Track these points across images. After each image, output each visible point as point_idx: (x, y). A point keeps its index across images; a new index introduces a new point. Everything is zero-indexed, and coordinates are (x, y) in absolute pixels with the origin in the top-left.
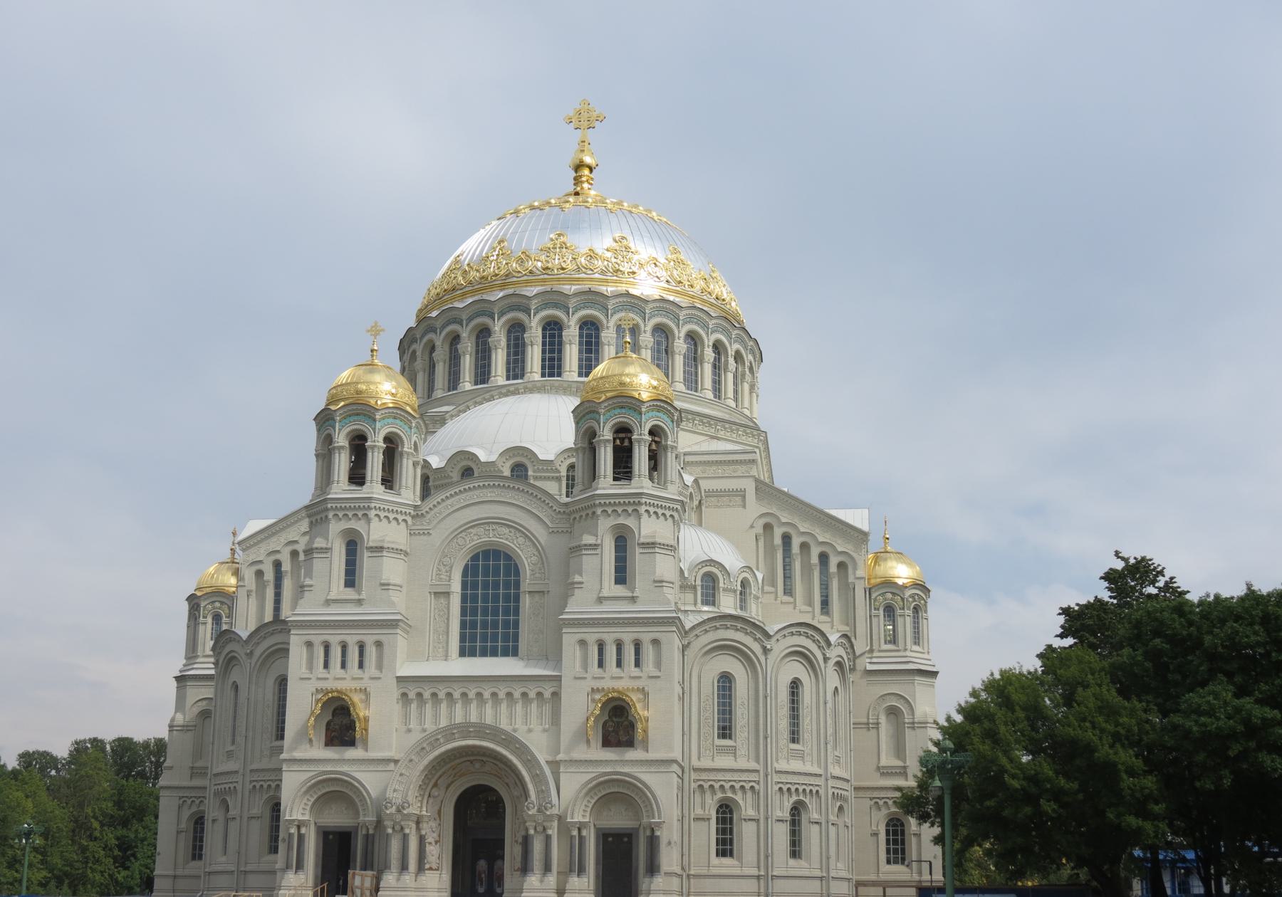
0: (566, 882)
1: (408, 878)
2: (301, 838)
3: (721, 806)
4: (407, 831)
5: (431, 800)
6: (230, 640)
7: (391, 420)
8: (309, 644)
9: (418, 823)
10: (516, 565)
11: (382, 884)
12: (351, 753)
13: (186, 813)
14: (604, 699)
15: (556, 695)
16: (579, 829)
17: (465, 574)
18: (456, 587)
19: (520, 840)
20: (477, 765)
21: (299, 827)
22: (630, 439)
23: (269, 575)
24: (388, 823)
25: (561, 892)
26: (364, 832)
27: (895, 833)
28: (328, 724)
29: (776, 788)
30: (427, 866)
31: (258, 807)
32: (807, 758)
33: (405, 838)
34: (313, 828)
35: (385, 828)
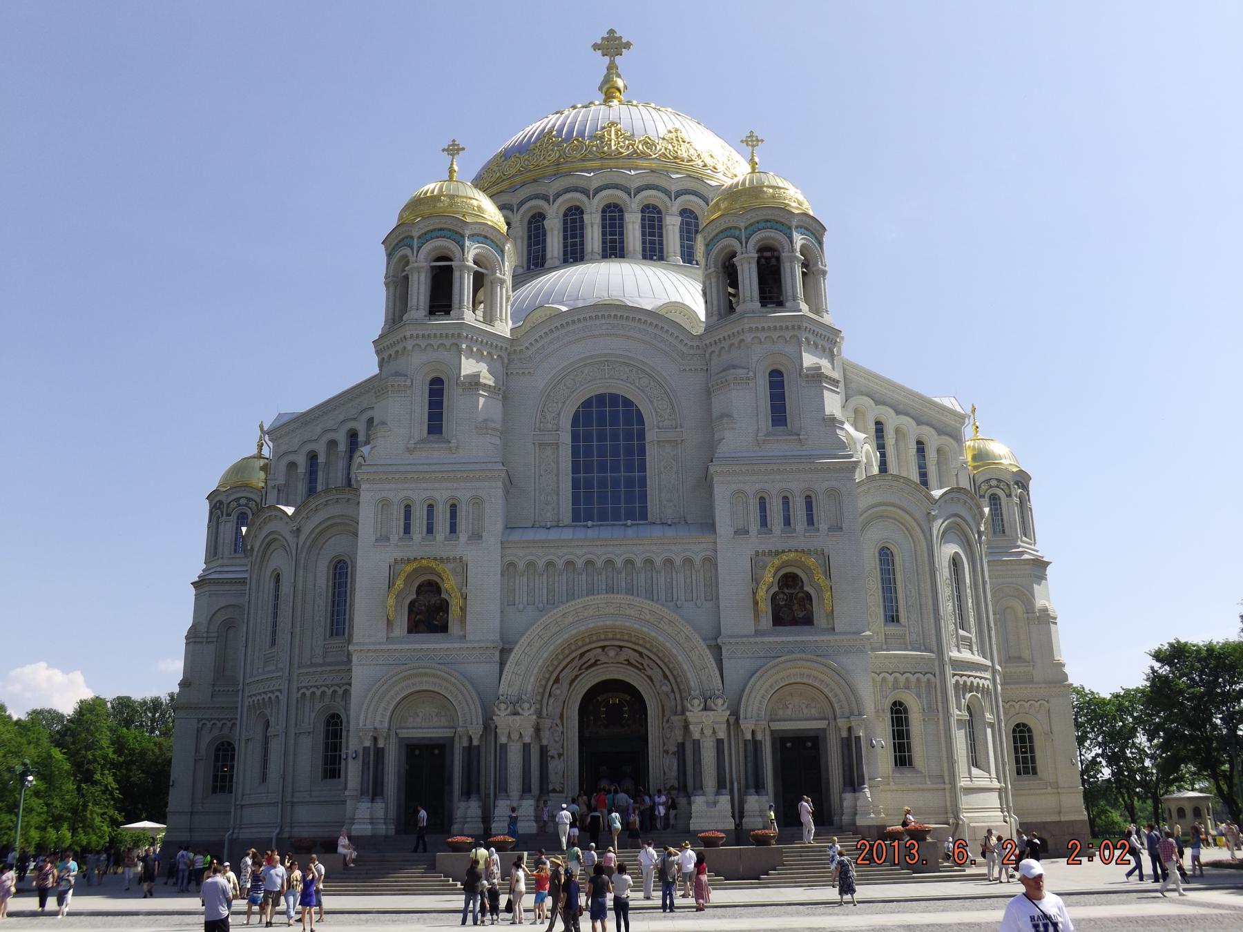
0: (742, 803)
2: (380, 753)
3: (895, 704)
5: (551, 700)
6: (270, 519)
7: (481, 239)
8: (385, 504)
9: (538, 730)
10: (638, 411)
13: (206, 739)
15: (711, 562)
17: (575, 422)
18: (566, 438)
19: (673, 749)
20: (612, 653)
21: (375, 739)
22: (778, 259)
23: (302, 469)
26: (465, 743)
27: (1023, 740)
28: (412, 604)
29: (953, 681)
30: (551, 787)
31: (312, 719)
32: (975, 648)
34: (393, 740)
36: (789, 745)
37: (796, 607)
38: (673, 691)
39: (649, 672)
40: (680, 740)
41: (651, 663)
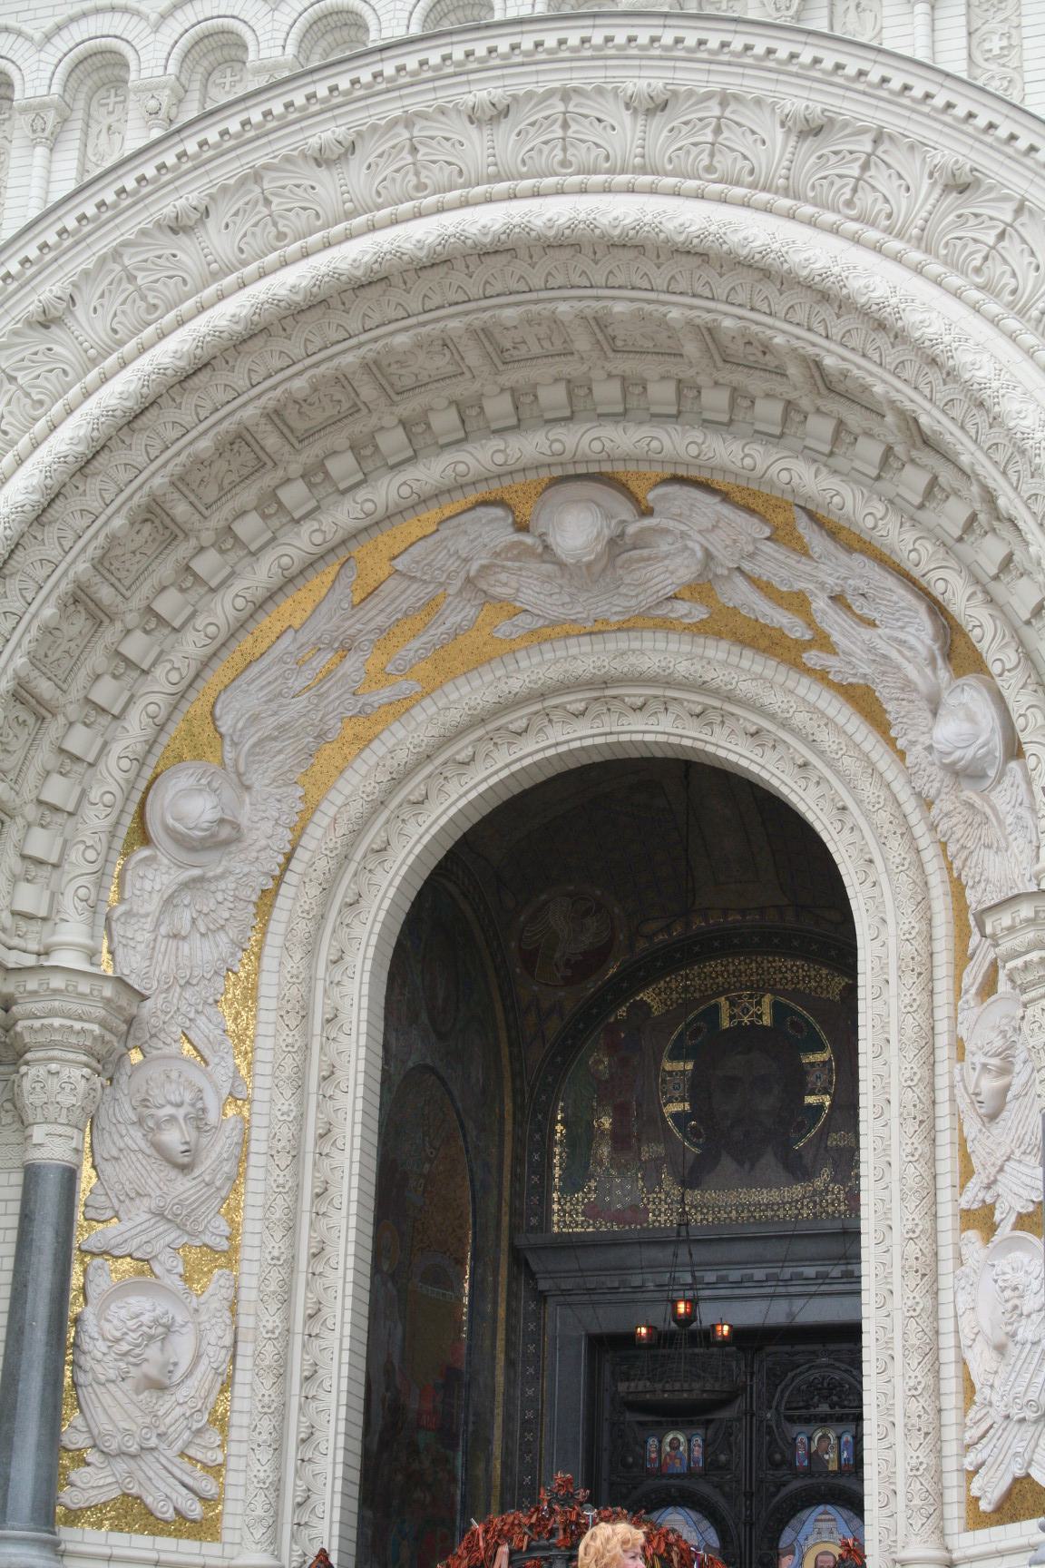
20: (577, 529)
30: (89, 1484)
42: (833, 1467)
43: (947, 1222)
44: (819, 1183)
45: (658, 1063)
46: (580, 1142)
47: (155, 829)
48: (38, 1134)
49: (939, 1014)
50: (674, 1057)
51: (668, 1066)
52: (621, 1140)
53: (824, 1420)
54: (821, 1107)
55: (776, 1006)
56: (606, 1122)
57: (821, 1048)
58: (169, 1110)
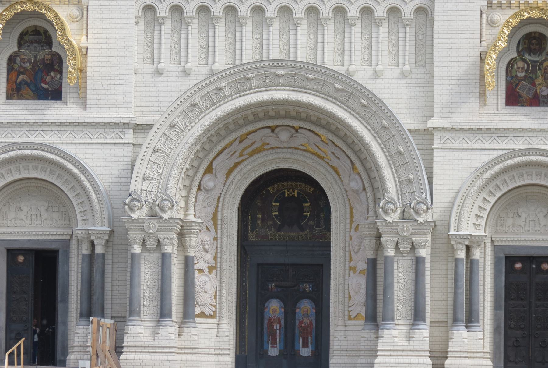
0: (447, 339)
1: (170, 329)
4: (168, 249)
9: (181, 235)
11: (127, 341)
12: (54, 111)
14: (515, 22)
16: (468, 248)
19: (362, 266)
20: (284, 135)
24: (134, 235)
25: (439, 357)
26: (85, 250)
28: (11, 60)
30: (197, 310)
33: (165, 259)
35: (127, 243)
36: (518, 266)
37: (539, 80)
38: (364, 189)
39: (335, 162)
40: (370, 254)
41: (337, 152)
42: (308, 291)
43: (347, 268)
44: (306, 232)
45: (271, 203)
46: (254, 220)
47: (202, 188)
48: (189, 250)
49: (347, 230)
50: (275, 202)
51: (274, 204)
52: (263, 220)
53: (306, 282)
54: (307, 216)
55: (298, 193)
56: (260, 216)
57: (308, 203)
58: (206, 242)
